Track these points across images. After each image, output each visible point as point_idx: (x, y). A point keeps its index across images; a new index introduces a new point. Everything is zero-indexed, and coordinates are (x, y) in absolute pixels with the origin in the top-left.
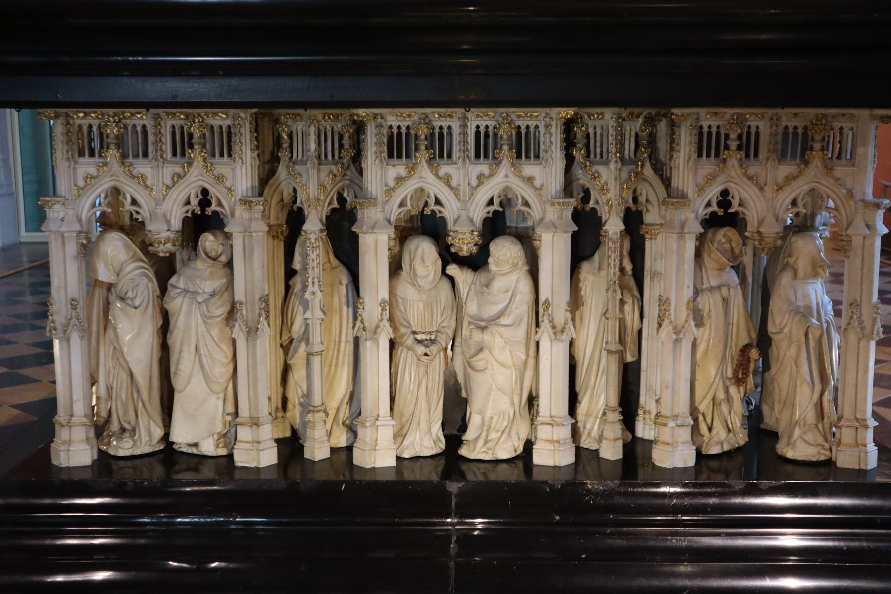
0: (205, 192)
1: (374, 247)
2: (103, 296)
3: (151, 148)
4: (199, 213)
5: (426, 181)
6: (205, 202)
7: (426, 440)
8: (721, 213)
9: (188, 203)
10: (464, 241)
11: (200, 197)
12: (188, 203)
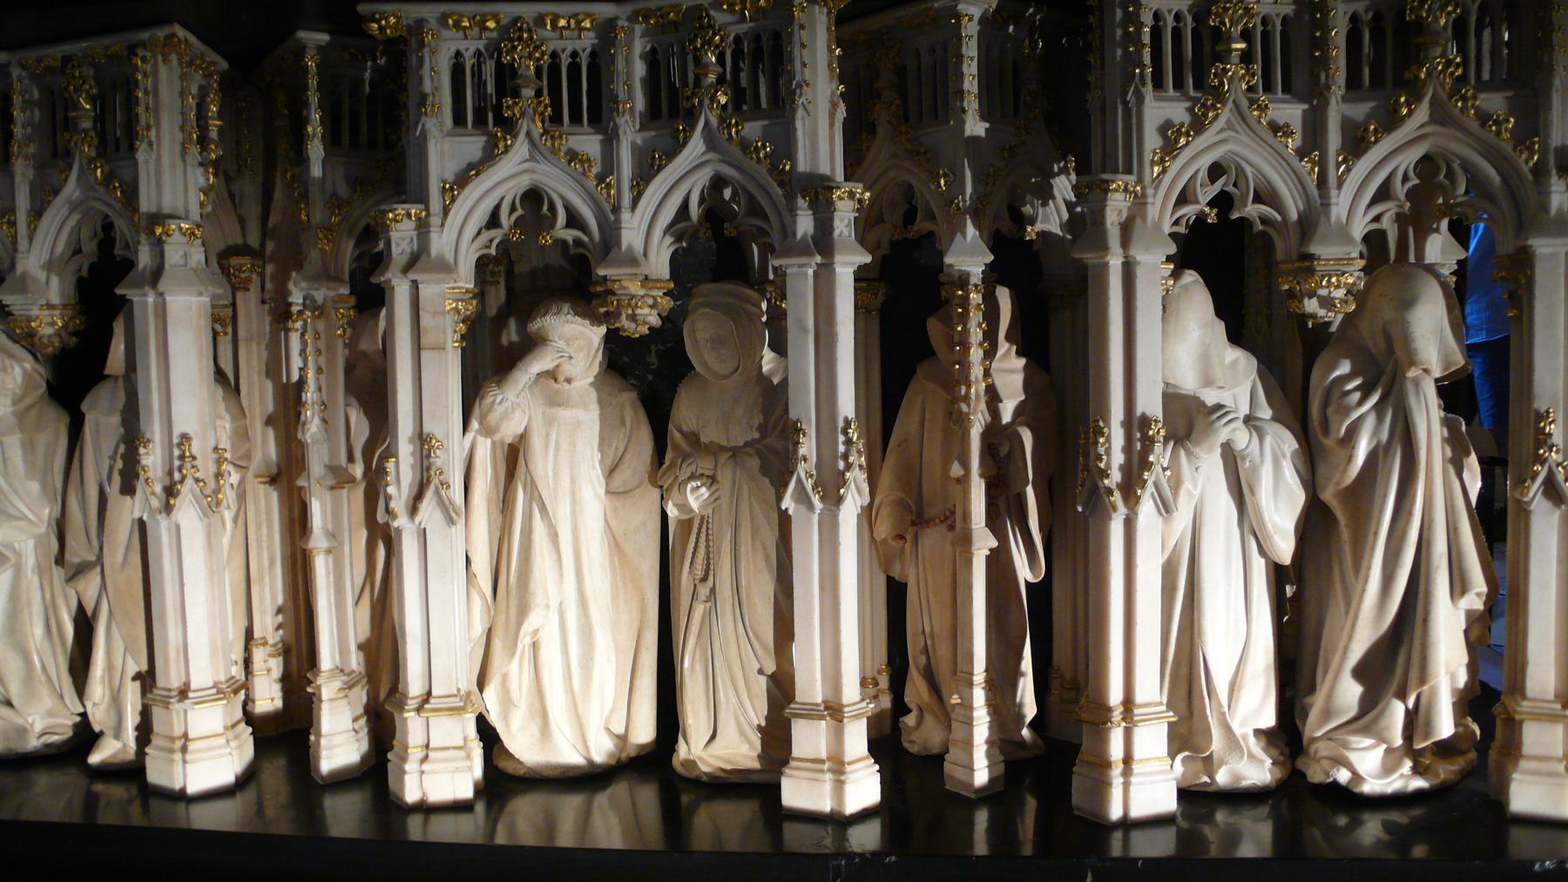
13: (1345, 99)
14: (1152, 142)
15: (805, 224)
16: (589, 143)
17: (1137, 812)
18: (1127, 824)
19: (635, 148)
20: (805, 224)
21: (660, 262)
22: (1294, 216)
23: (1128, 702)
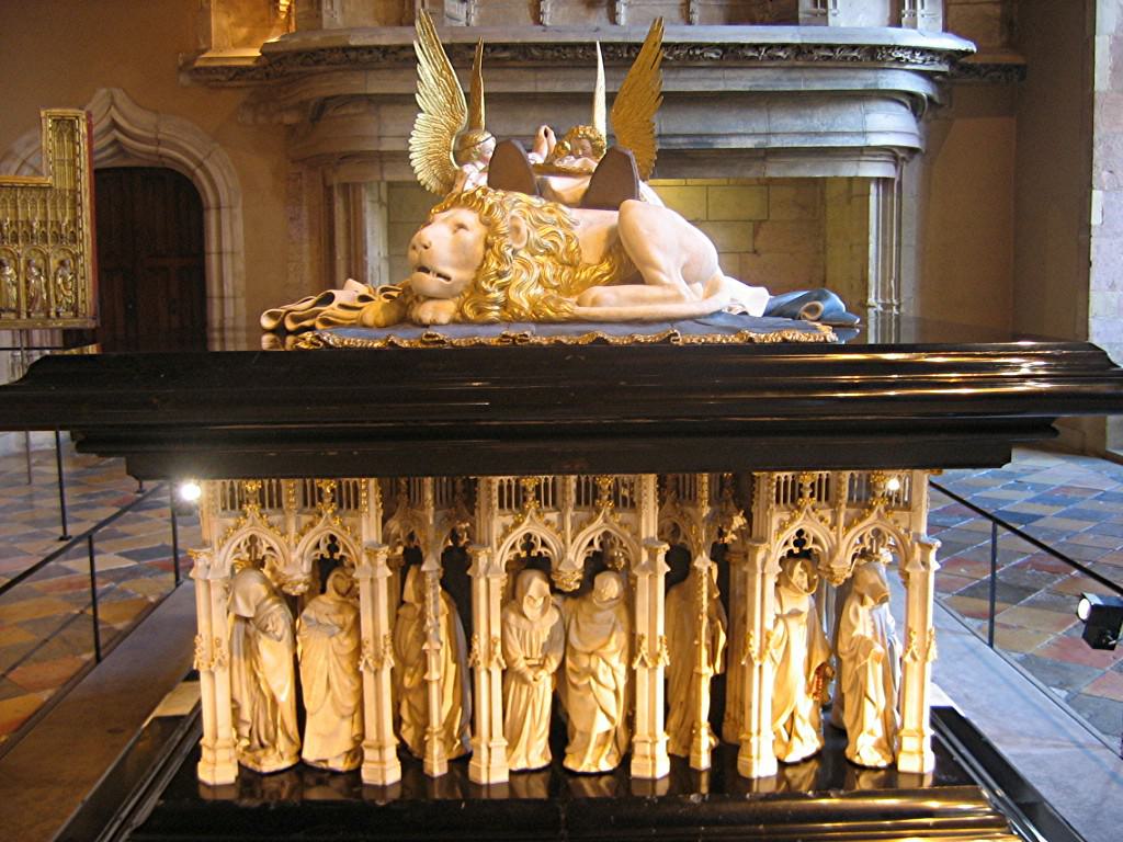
0: (333, 538)
1: (488, 587)
2: (249, 630)
3: (284, 500)
4: (328, 557)
5: (537, 525)
6: (333, 548)
7: (535, 754)
8: (796, 551)
9: (317, 546)
10: (571, 578)
11: (329, 542)
12: (317, 546)
13: (847, 506)
14: (775, 526)
15: (645, 557)
16: (553, 516)
17: (763, 775)
18: (759, 778)
19: (573, 518)
20: (645, 557)
21: (580, 564)
22: (827, 549)
23: (759, 732)
